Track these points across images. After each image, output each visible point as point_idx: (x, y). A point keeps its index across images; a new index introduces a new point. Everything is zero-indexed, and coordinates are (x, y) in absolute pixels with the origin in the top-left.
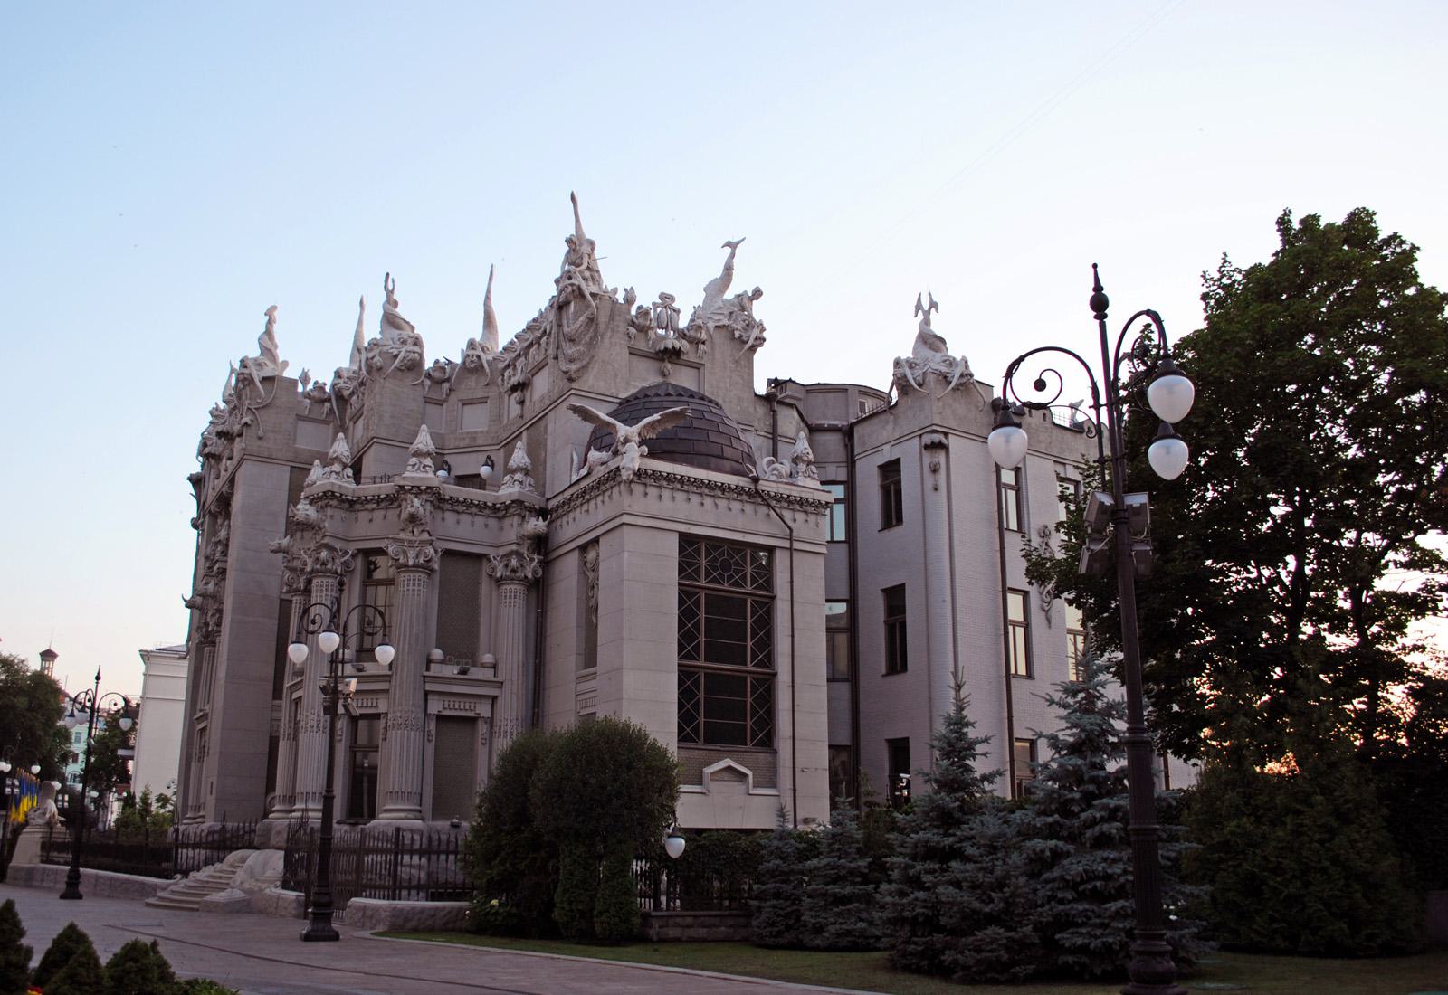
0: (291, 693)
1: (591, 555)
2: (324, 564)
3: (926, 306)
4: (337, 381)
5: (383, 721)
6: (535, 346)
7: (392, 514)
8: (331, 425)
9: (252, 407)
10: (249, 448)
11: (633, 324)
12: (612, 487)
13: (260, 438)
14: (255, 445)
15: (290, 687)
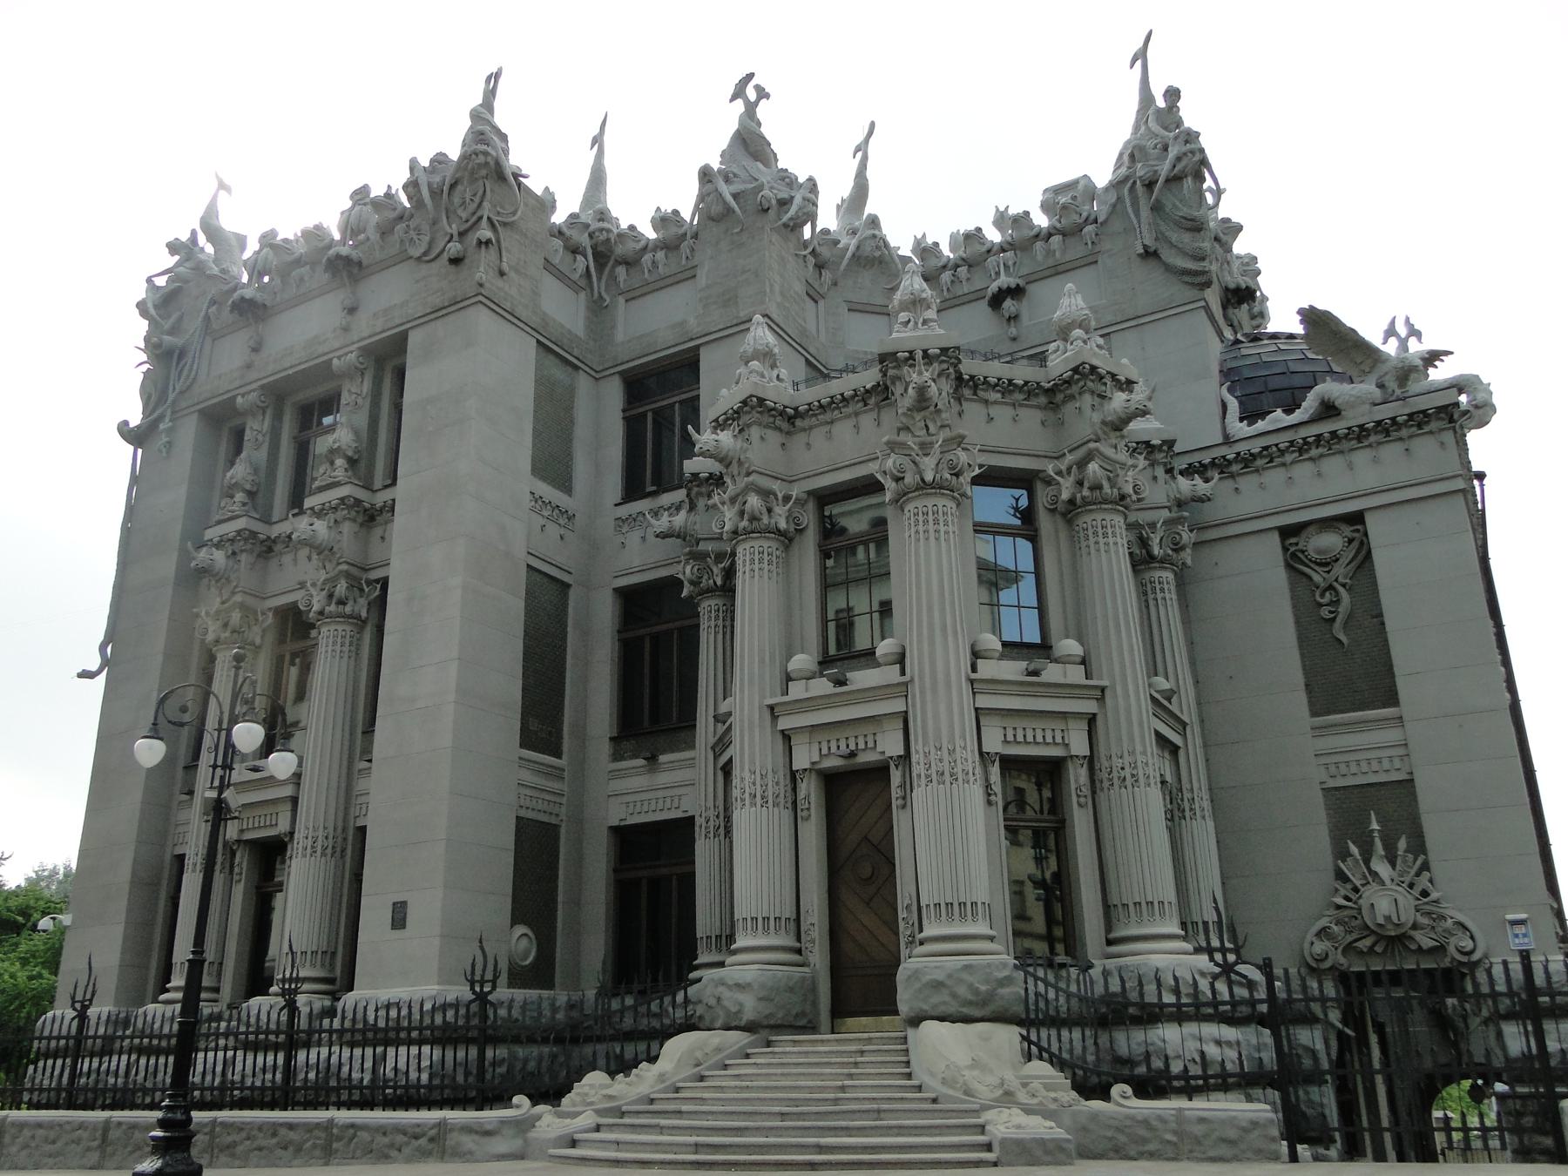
0: (774, 718)
1: (1330, 541)
2: (957, 475)
3: (1402, 330)
4: (605, 225)
5: (1077, 777)
6: (1056, 239)
7: (1031, 418)
8: (582, 295)
9: (495, 218)
10: (487, 285)
11: (1216, 239)
12: (1411, 437)
13: (502, 274)
14: (494, 284)
15: (772, 708)
